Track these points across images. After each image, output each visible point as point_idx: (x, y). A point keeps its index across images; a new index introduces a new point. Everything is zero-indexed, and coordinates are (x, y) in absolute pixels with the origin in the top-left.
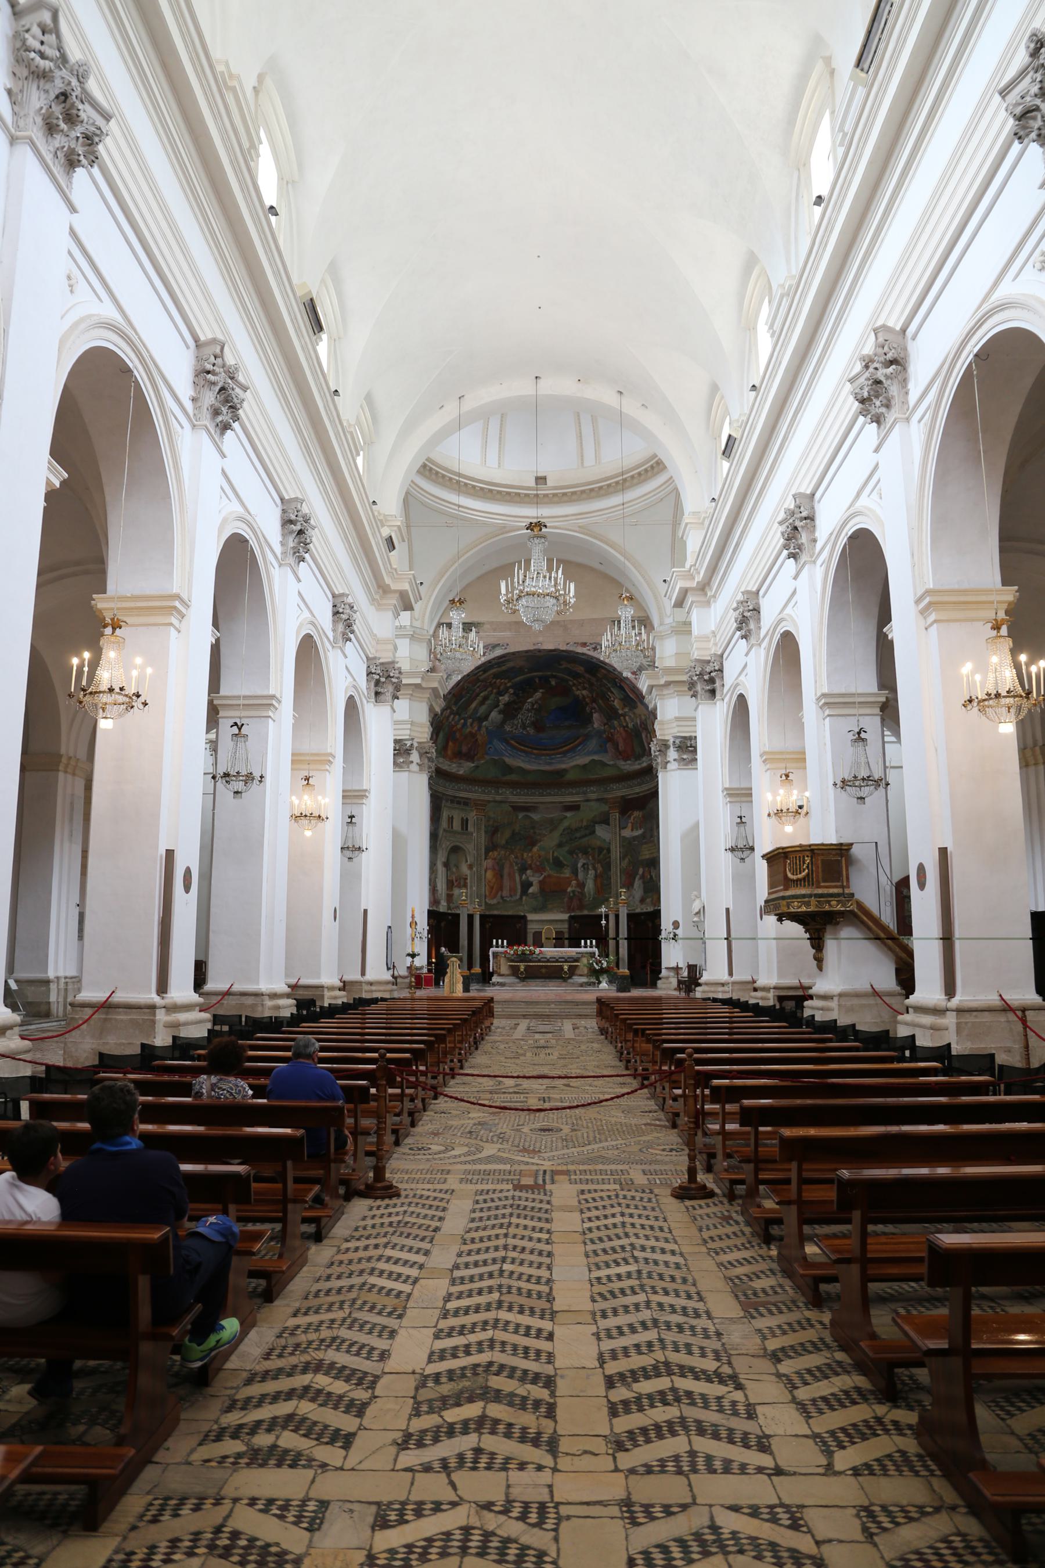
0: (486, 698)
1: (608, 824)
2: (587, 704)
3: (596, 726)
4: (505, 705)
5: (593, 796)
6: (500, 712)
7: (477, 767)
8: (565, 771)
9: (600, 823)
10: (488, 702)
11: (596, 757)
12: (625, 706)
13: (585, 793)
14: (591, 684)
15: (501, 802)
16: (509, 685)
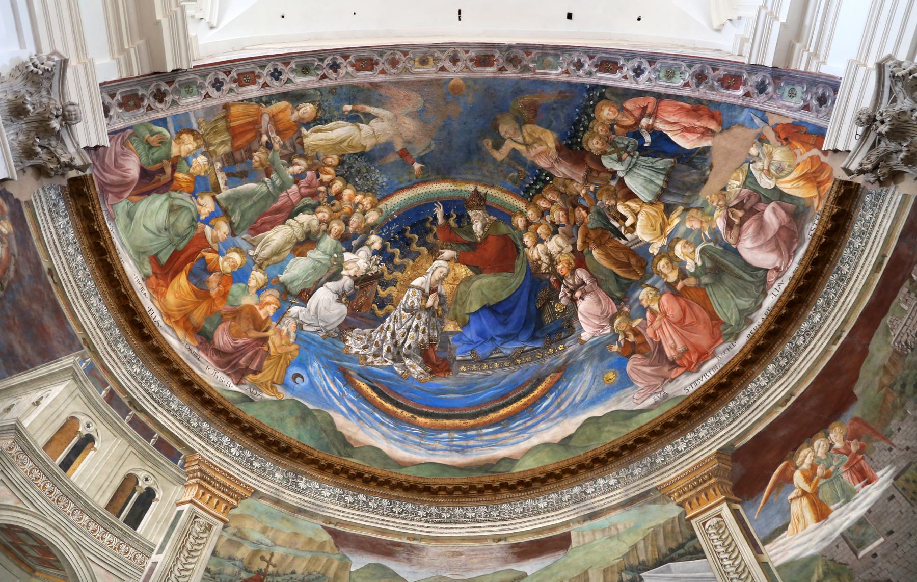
0: (308, 241)
1: (697, 553)
2: (560, 279)
3: (586, 335)
4: (357, 280)
5: (618, 496)
6: (341, 296)
7: (247, 399)
8: (510, 461)
9: (659, 563)
10: (315, 255)
11: (598, 411)
12: (669, 210)
13: (577, 500)
14: (572, 202)
15: (300, 511)
16: (373, 217)
